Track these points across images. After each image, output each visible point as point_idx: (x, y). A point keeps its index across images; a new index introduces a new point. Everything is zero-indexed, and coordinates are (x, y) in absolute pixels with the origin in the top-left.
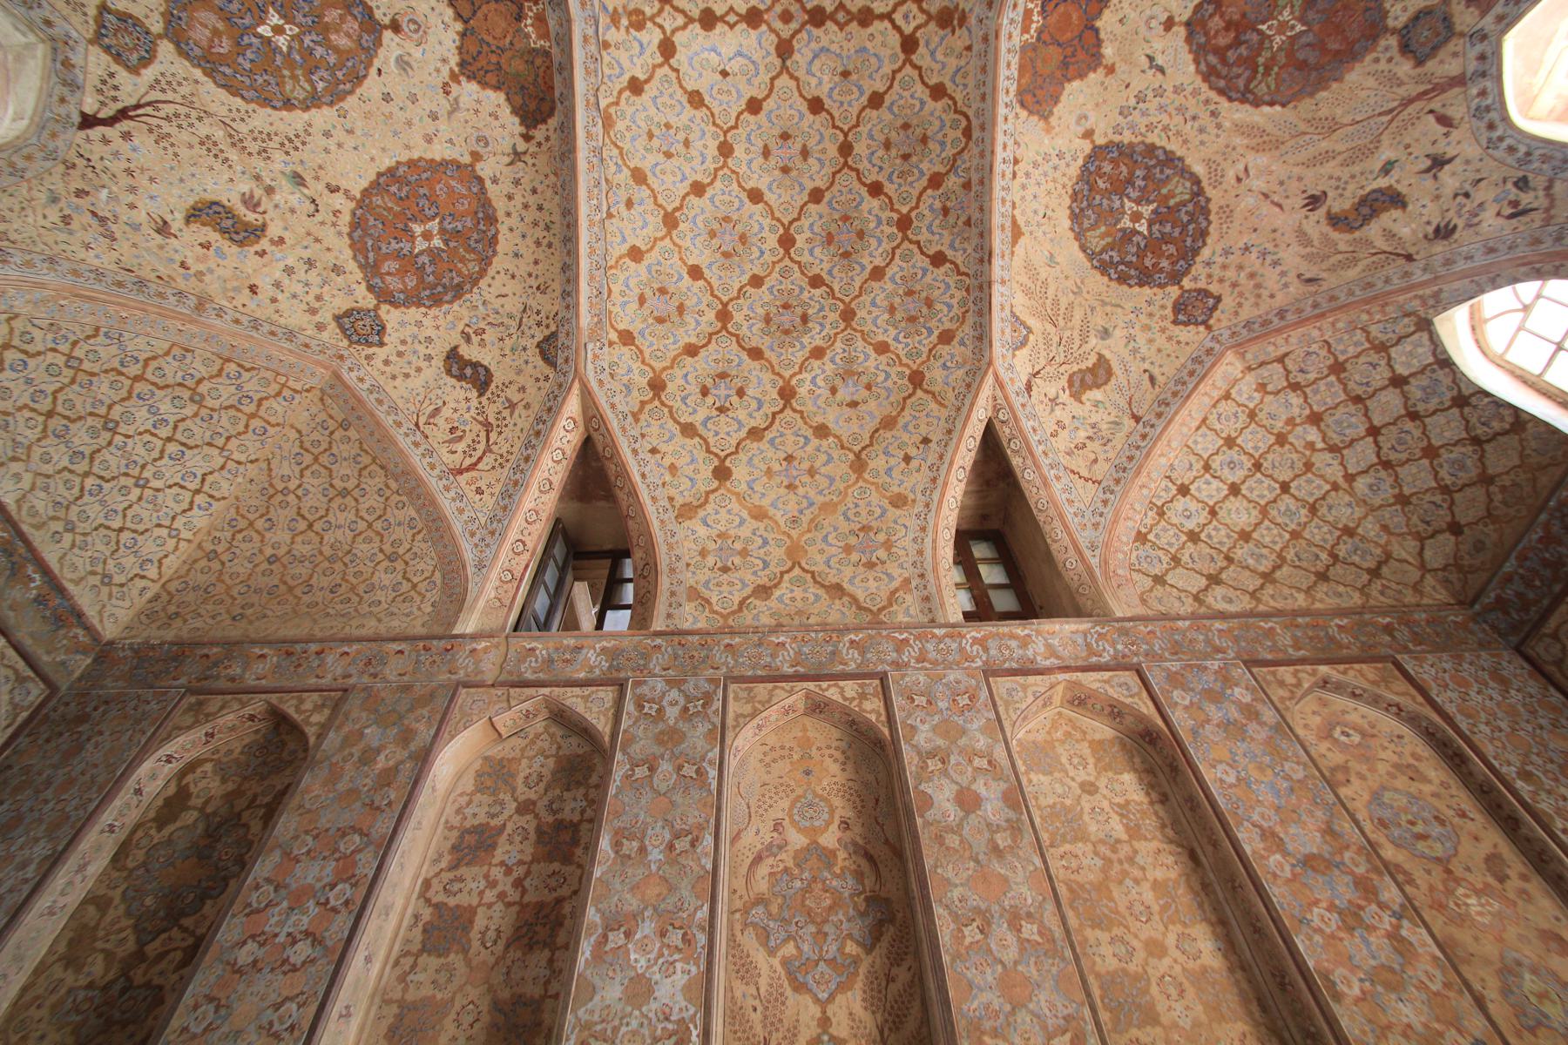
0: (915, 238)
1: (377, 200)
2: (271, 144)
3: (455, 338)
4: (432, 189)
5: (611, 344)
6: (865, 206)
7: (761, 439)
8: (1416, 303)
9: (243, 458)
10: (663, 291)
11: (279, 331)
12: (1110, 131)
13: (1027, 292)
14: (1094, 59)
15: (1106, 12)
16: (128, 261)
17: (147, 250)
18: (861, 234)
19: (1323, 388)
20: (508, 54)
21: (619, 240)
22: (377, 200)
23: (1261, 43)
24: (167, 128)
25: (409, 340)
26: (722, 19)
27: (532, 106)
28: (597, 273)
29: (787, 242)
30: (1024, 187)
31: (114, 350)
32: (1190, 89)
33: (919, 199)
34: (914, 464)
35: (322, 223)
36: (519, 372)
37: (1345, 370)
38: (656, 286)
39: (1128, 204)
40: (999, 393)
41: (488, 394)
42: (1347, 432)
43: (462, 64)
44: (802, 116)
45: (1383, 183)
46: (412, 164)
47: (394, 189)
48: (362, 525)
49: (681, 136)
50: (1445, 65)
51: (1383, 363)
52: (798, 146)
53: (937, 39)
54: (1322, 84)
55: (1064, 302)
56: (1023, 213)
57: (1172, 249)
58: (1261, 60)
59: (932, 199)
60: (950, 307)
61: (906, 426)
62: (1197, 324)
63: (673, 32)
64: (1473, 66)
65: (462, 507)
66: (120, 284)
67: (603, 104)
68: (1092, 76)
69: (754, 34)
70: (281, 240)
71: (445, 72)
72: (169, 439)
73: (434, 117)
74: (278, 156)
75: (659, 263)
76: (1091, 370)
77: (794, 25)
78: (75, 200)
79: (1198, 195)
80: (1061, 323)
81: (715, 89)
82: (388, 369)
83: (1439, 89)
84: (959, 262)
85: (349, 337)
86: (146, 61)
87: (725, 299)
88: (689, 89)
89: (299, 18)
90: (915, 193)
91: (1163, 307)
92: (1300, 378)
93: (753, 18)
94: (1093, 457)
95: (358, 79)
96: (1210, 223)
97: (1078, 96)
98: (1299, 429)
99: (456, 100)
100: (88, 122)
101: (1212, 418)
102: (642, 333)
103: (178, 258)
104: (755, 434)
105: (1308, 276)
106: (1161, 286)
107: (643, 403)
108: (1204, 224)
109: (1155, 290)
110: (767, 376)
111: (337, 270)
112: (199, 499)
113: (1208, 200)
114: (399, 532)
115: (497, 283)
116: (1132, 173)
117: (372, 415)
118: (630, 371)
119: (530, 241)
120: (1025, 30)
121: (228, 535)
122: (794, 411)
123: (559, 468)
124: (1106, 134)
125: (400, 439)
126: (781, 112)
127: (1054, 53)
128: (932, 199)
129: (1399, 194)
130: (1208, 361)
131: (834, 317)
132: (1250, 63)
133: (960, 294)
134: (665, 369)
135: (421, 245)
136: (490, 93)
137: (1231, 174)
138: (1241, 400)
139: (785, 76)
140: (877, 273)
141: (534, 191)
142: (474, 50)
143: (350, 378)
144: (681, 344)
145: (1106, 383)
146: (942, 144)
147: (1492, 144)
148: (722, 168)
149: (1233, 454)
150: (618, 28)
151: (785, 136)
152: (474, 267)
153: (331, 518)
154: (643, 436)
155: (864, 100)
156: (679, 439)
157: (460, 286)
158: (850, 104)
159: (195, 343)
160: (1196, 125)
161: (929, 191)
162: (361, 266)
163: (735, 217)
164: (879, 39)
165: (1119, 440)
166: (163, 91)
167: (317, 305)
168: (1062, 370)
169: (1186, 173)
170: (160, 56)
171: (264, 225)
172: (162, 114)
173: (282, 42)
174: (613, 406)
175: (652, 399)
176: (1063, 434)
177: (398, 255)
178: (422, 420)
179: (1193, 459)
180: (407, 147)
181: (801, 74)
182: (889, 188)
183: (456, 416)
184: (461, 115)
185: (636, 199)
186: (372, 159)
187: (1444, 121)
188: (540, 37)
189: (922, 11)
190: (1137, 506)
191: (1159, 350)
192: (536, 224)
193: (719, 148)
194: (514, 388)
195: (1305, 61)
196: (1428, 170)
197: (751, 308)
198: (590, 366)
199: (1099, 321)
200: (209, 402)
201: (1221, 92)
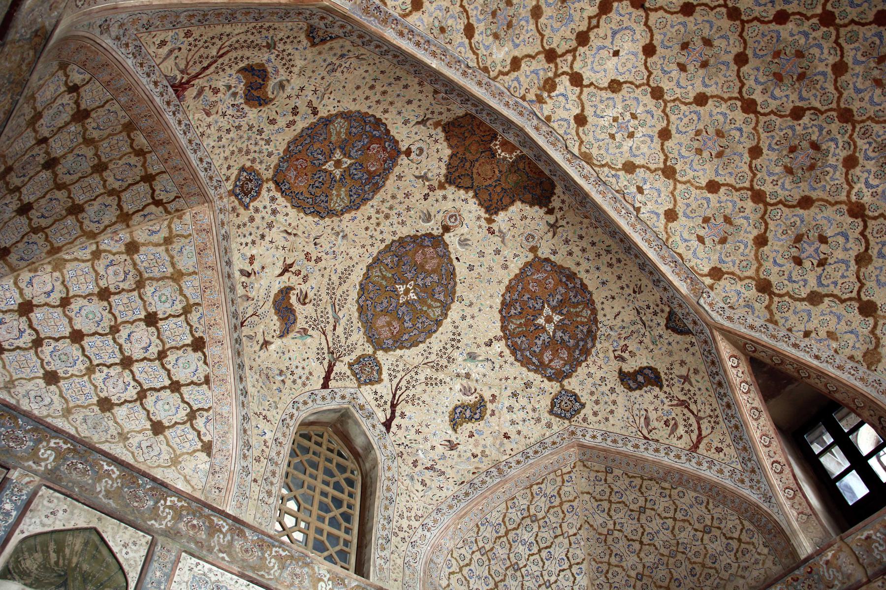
1: (512, 327)
2: (449, 351)
3: (615, 365)
4: (529, 291)
5: (711, 287)
6: (784, 34)
7: (870, 259)
9: (574, 531)
10: (706, 220)
11: (536, 447)
16: (458, 479)
17: (457, 463)
20: (503, 179)
22: (512, 327)
24: (411, 393)
25: (594, 389)
26: (590, 29)
28: (663, 252)
29: (749, 106)
31: (489, 529)
35: (501, 367)
36: (670, 354)
41: (665, 383)
43: (487, 211)
44: (684, 24)
46: (509, 289)
47: (513, 312)
48: (670, 522)
49: (628, 116)
52: (699, 43)
63: (571, 68)
65: (717, 467)
66: (467, 494)
67: (576, 152)
69: (612, 15)
70: (493, 396)
71: (484, 223)
72: (540, 551)
73: (497, 252)
74: (456, 354)
75: (688, 205)
78: (416, 470)
82: (599, 417)
85: (565, 418)
86: (380, 372)
87: (747, 185)
88: (606, 85)
89: (409, 275)
95: (453, 274)
99: (500, 231)
100: (387, 425)
102: (721, 261)
103: (469, 454)
104: (862, 259)
107: (768, 308)
110: (830, 211)
111: (528, 385)
112: (575, 569)
114: (697, 512)
115: (608, 310)
117: (619, 453)
118: (739, 293)
119: (604, 268)
121: (603, 578)
122: (875, 218)
123: (752, 395)
125: (645, 454)
131: (835, 126)
134: (757, 270)
135: (550, 328)
136: (512, 208)
140: (840, 68)
141: (581, 237)
142: (486, 197)
143: (588, 441)
144: (750, 243)
148: (665, 106)
150: (546, 103)
151: (685, 46)
152: (587, 313)
153: (648, 530)
154: (790, 330)
156: (815, 310)
157: (589, 331)
159: (514, 491)
162: (536, 371)
166: (395, 377)
167: (536, 415)
170: (382, 362)
171: (481, 397)
172: (404, 389)
173: (412, 296)
174: (752, 327)
175: (771, 299)
177: (545, 347)
178: (645, 432)
180: (500, 282)
183: (660, 413)
184: (508, 237)
186: (491, 307)
188: (511, 153)
192: (599, 255)
193: (653, 97)
194: (677, 366)
197: (770, 174)
198: (714, 314)
200: (540, 515)
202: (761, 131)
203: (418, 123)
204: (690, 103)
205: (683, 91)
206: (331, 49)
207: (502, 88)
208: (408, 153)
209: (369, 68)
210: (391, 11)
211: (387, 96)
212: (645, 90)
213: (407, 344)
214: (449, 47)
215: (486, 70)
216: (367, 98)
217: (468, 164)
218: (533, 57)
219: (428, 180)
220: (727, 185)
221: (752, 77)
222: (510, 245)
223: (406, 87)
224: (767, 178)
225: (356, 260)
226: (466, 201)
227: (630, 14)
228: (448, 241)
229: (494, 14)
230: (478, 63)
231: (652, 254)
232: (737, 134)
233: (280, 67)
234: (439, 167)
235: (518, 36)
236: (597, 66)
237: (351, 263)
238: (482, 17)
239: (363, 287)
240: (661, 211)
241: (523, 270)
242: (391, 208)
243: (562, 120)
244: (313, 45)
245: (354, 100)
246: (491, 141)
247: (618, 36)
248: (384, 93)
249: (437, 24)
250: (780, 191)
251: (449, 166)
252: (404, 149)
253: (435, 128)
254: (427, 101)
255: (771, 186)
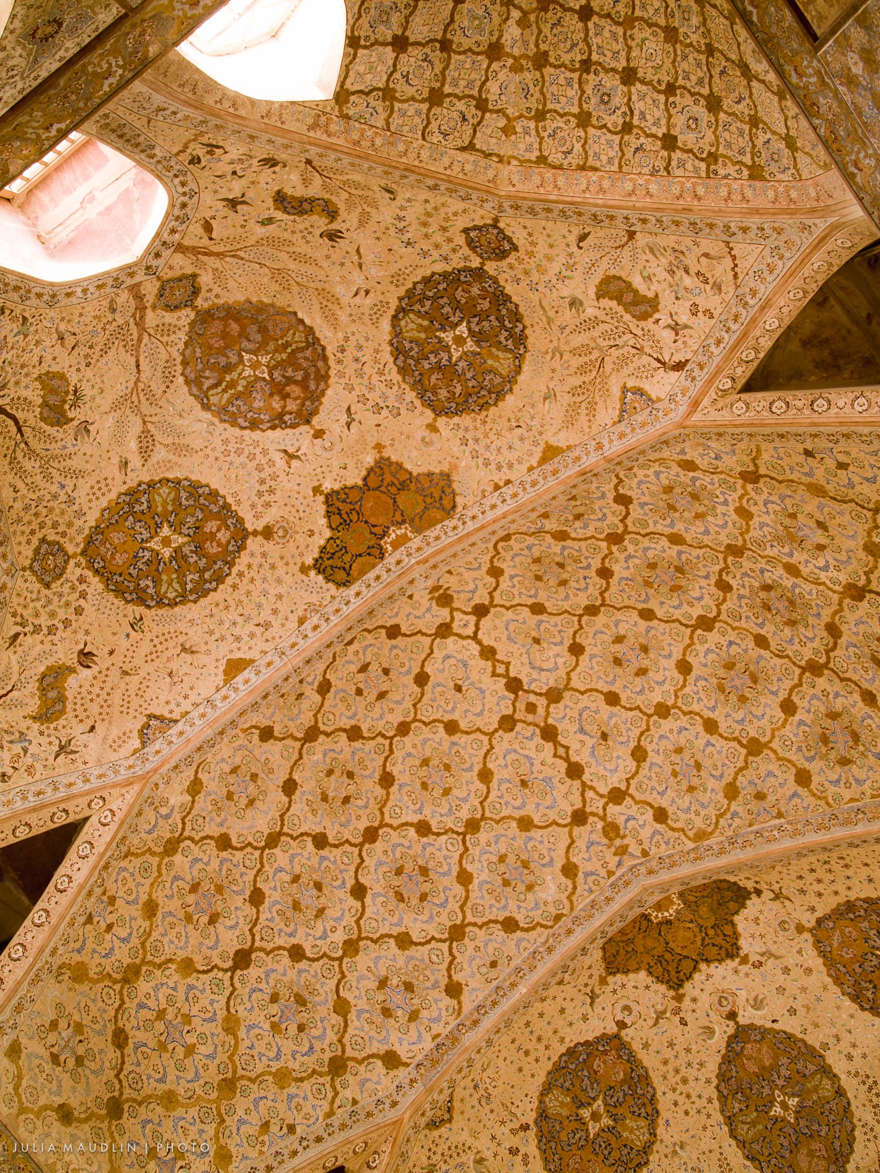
0: (621, 525)
6: (626, 574)
8: (333, 127)
10: (824, 740)
12: (417, 412)
13: (592, 408)
14: (382, 466)
15: (350, 483)
18: (652, 566)
19: (462, 83)
20: (701, 922)
21: (796, 800)
23: (275, 367)
26: (567, 759)
27: (729, 894)
28: (840, 816)
30: (510, 466)
32: (342, 381)
33: (586, 539)
34: (842, 458)
37: (432, 90)
38: (824, 750)
39: (456, 356)
40: (706, 402)
42: (481, 12)
43: (731, 956)
44: (592, 657)
45: (279, 215)
46: (838, 982)
47: (869, 994)
49: (676, 758)
50: (182, 264)
51: (398, 75)
52: (618, 647)
53: (462, 595)
54: (261, 308)
55: (576, 362)
56: (530, 454)
57: (459, 294)
58: (284, 356)
59: (577, 530)
60: (657, 474)
61: (806, 474)
62: (501, 231)
63: (602, 796)
64: (166, 253)
68: (394, 458)
69: (560, 728)
76: (619, 300)
77: (532, 698)
79: (404, 310)
80: (596, 354)
81: (621, 739)
83: (195, 251)
84: (612, 486)
87: (798, 671)
88: (635, 764)
89: (766, 1091)
90: (583, 544)
91: (511, 267)
92: (472, 112)
93: (549, 734)
94: (703, 260)
95: (789, 1037)
96: (415, 284)
97: (416, 461)
98: (516, 52)
99: (762, 955)
101: (574, 160)
105: (388, 195)
106: (495, 281)
108: (420, 287)
109: (502, 283)
113: (400, 299)
116: (432, 370)
119: (850, 872)
120: (404, 539)
124: (422, 413)
126: (601, 674)
127: (402, 499)
128: (577, 530)
129: (275, 201)
130: (525, 204)
132: (292, 362)
133: (640, 473)
136: (740, 928)
137: (368, 301)
138: (533, 139)
139: (573, 684)
140: (676, 539)
141: (801, 877)
144: (868, 710)
145: (620, 278)
146: (529, 548)
147: (192, 194)
148: (679, 708)
149: (592, 105)
150: (627, 846)
151: (618, 662)
155: (544, 617)
158: (556, 625)
160: (359, 354)
161: (573, 535)
163: (715, 681)
164: (494, 634)
165: (668, 240)
168: (639, 332)
169: (396, 331)
173: (793, 1102)
176: (703, 304)
179: (629, 152)
180: (825, 988)
181: (562, 672)
182: (596, 564)
184: (774, 949)
185: (751, 790)
186: (852, 1016)
187: (208, 227)
188: (673, 903)
189: (452, 618)
190: (724, 192)
191: (551, 246)
193: (666, 718)
195: (259, 331)
196: (244, 203)
199: (568, 316)
201: (325, 359)
202: (737, 624)
203: (591, 1004)
204: (685, 680)
205: (668, 681)
206: (462, 1100)
207: (588, 901)
208: (622, 1025)
209: (502, 1055)
210: (449, 1028)
211: (544, 1037)
212: (655, 722)
213: (846, 1150)
214: (513, 964)
215: (558, 918)
216: (537, 1061)
217: (668, 956)
218: (573, 842)
219: (665, 1012)
220: (791, 690)
221: (671, 610)
222: (782, 952)
223: (541, 1015)
224: (795, 648)
225: (715, 1147)
226: (709, 977)
227: (566, 707)
228: (748, 1022)
229: (506, 883)
230: (546, 927)
231: (839, 833)
232: (734, 650)
233: (459, 1160)
234: (656, 992)
235: (542, 856)
236: (608, 770)
237: (715, 1156)
238: (503, 901)
239: (752, 1158)
240: (792, 786)
241: (822, 954)
242: (677, 1071)
243: (652, 837)
244: (450, 1120)
245: (533, 1076)
246: (650, 921)
247: (587, 728)
248: (539, 1039)
249: (484, 970)
250: (814, 645)
251: (659, 980)
252: (615, 1029)
253: (607, 984)
254: (569, 991)
255: (805, 649)
